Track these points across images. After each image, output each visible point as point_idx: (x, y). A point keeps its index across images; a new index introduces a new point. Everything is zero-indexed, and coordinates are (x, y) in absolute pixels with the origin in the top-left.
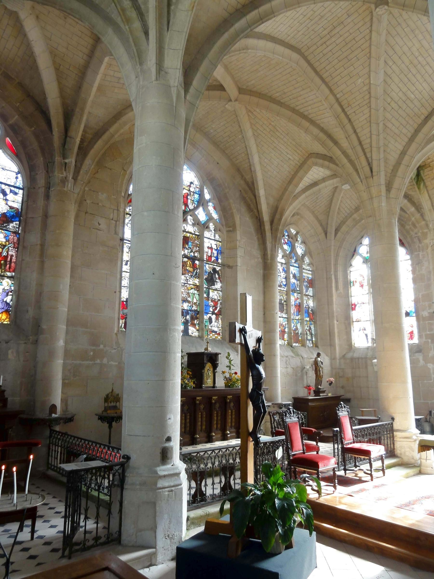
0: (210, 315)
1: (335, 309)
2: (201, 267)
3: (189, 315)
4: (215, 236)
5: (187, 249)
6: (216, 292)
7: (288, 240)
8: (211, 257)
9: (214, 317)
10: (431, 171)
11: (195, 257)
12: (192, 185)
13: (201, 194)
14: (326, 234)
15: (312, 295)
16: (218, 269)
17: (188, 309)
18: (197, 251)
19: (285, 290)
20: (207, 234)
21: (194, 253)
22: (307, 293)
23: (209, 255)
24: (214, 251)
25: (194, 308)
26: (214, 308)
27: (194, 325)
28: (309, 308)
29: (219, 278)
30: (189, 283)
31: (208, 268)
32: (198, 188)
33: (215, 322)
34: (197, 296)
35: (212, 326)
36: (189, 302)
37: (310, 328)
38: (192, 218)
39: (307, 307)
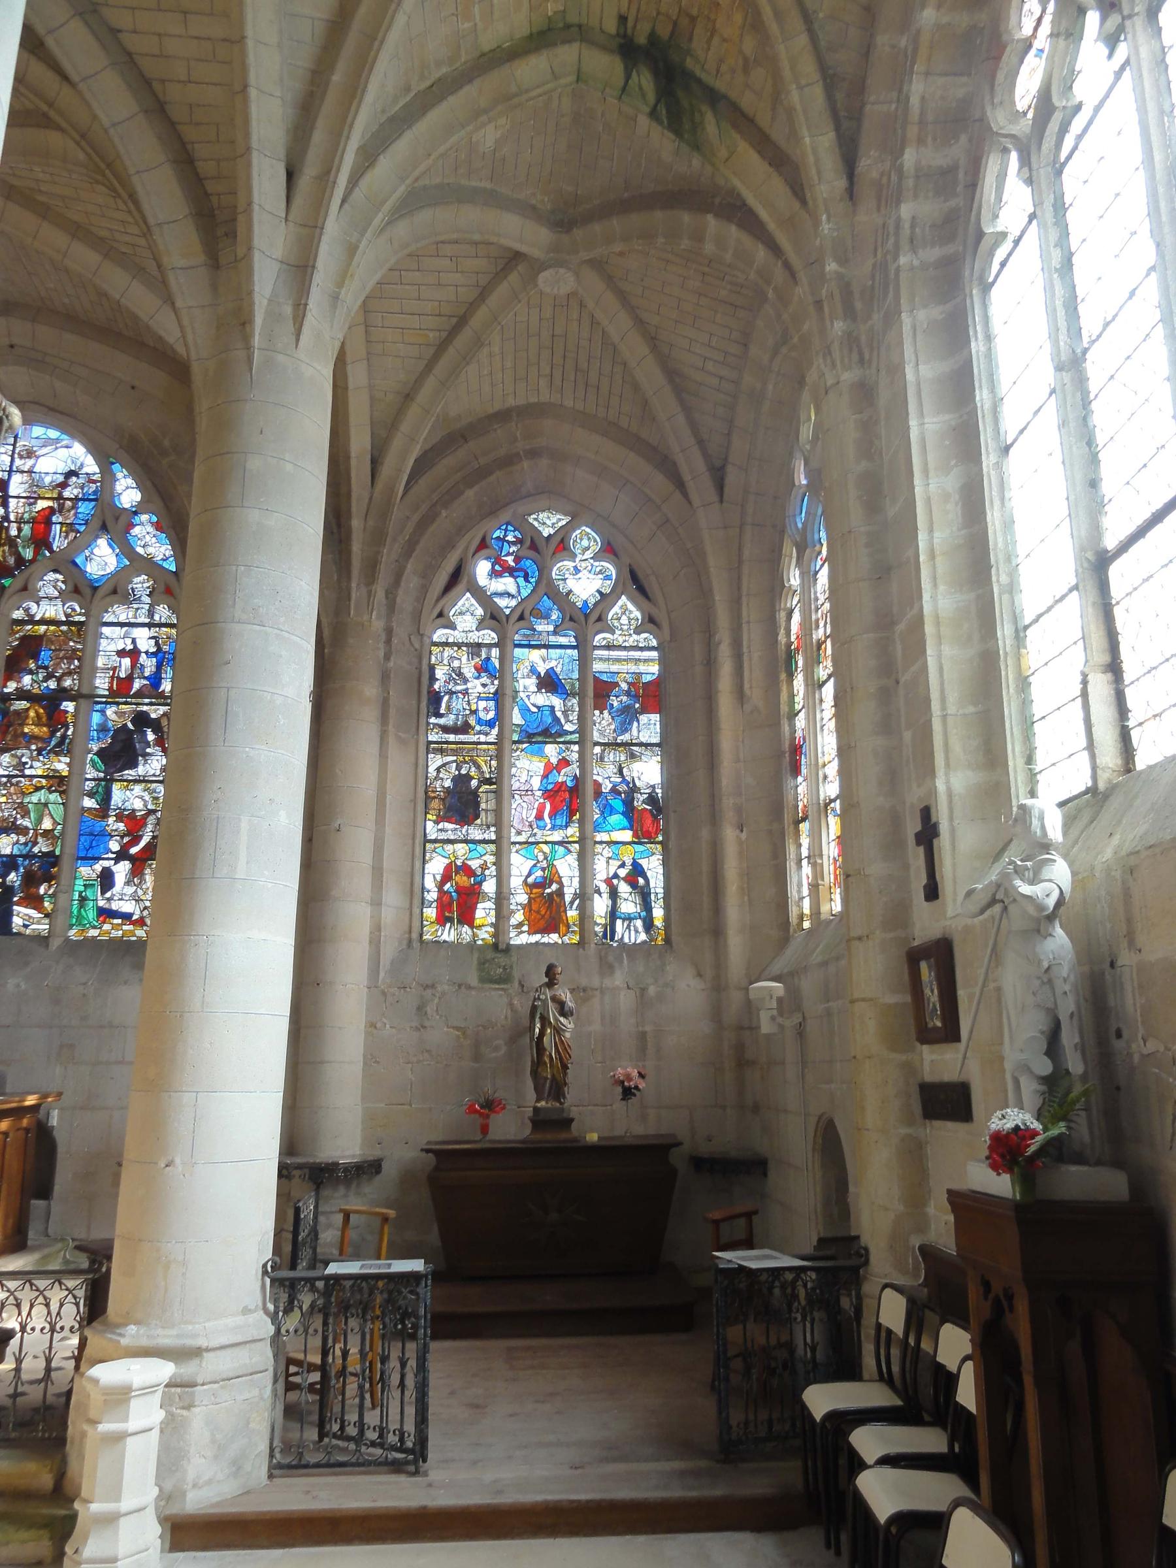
0: (106, 864)
1: (725, 782)
3: (17, 870)
4: (151, 614)
5: (31, 672)
6: (138, 789)
7: (517, 560)
8: (130, 679)
9: (122, 870)
10: (716, 41)
11: (64, 690)
12: (74, 479)
13: (103, 497)
14: (685, 494)
15: (656, 740)
16: (156, 712)
17: (16, 852)
18: (69, 673)
19: (492, 738)
21: (59, 680)
22: (625, 737)
23: (123, 675)
24: (143, 658)
25: (42, 847)
26: (126, 840)
27: (34, 901)
28: (633, 789)
29: (160, 742)
30: (27, 772)
32: (94, 482)
33: (128, 883)
34: (58, 812)
35: (109, 900)
36: (23, 831)
37: (637, 871)
38: (61, 577)
39: (622, 788)
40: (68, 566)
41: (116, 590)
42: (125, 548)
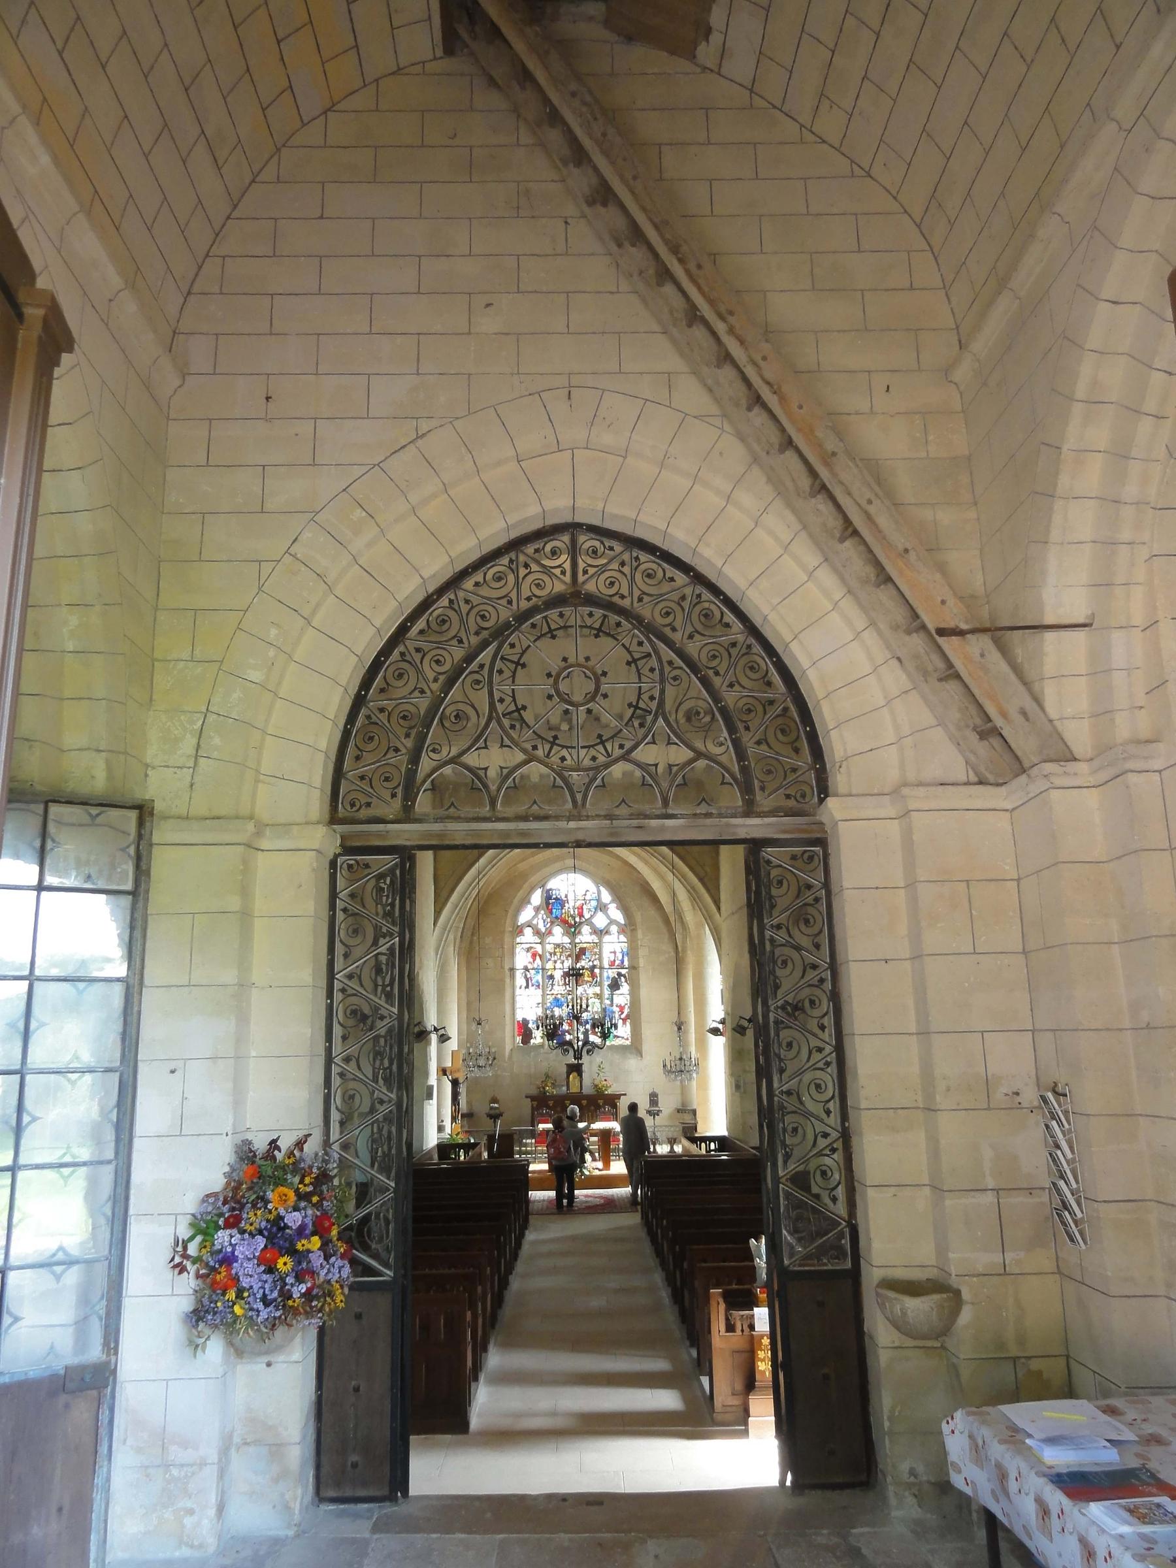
2: (601, 974)
13: (599, 900)
16: (623, 971)
20: (606, 938)
27: (595, 1033)
31: (612, 973)
40: (589, 922)
41: (607, 932)
42: (608, 917)
